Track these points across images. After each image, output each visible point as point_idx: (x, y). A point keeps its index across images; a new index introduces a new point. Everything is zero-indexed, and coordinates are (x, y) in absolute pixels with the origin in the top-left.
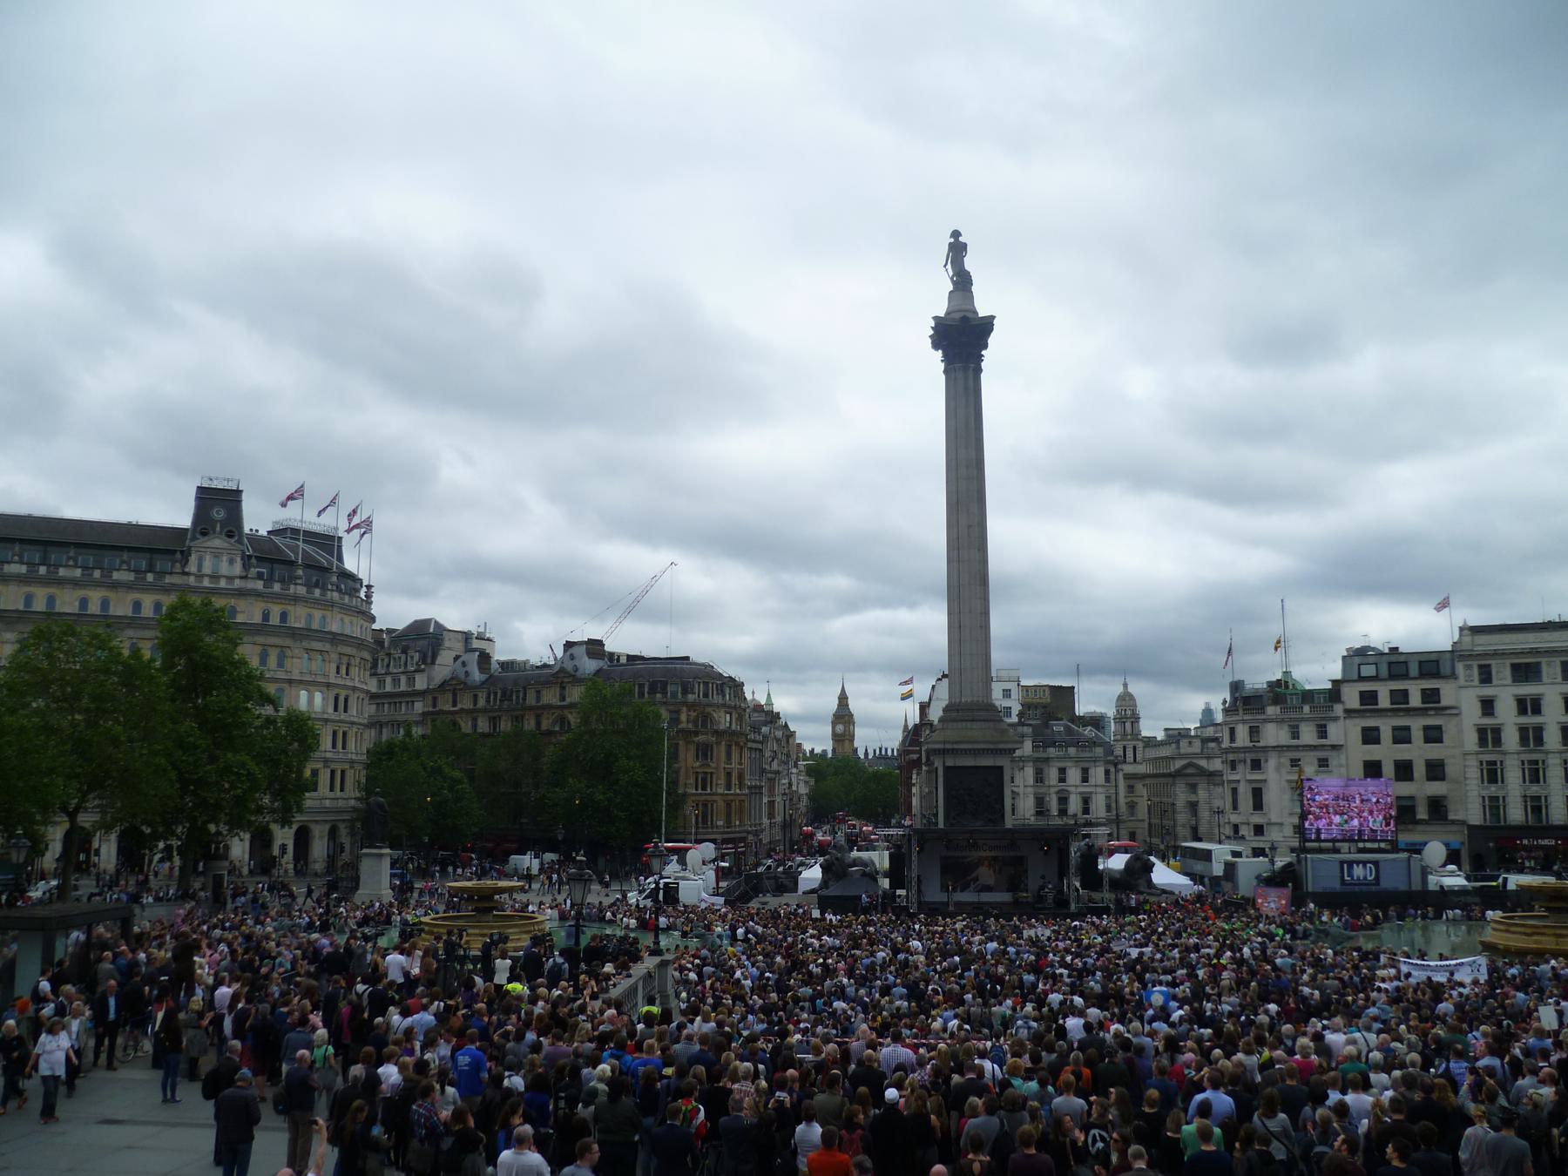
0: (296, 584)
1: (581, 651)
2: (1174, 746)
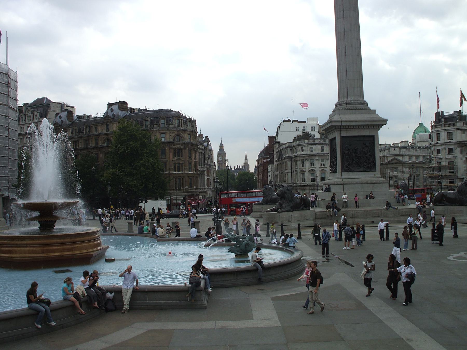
1: (115, 108)
2: (387, 151)
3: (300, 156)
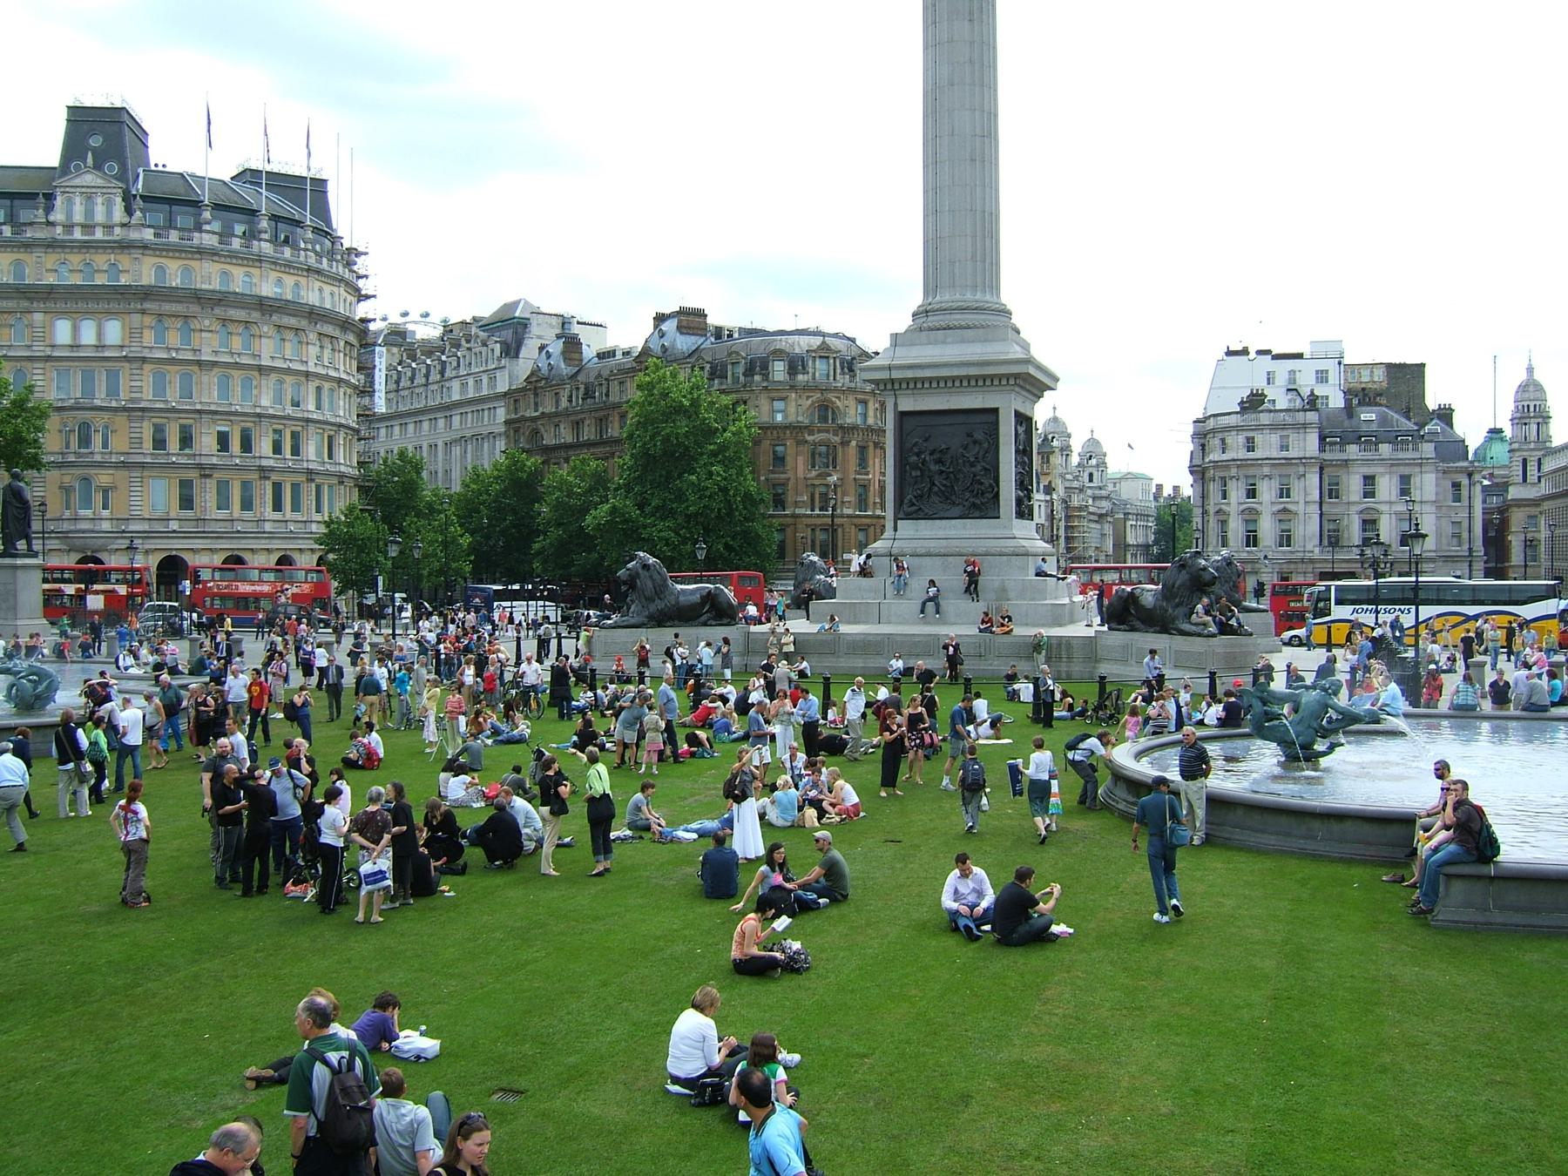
0: (201, 231)
1: (669, 326)
3: (1216, 465)
